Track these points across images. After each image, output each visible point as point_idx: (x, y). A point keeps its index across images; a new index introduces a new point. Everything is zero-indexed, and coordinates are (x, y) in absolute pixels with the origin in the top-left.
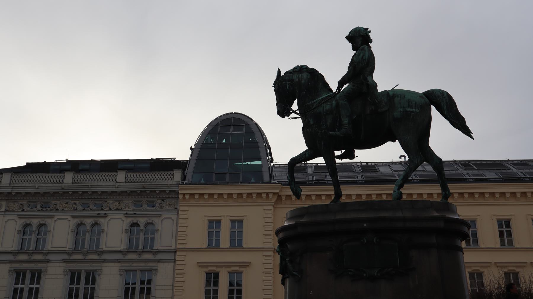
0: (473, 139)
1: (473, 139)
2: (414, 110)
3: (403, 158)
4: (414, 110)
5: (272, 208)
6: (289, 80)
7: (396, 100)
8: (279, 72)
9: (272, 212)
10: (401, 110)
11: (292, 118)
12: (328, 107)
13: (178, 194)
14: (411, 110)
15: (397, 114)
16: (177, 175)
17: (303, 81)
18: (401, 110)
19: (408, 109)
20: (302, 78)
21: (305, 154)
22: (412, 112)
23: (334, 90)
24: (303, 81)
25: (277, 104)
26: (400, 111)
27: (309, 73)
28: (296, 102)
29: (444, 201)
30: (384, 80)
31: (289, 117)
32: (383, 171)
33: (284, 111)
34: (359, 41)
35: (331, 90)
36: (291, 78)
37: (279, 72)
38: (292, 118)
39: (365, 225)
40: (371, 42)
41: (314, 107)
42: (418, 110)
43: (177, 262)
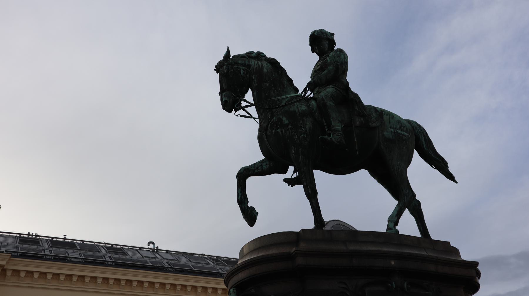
0: (456, 182)
1: (456, 182)
2: (406, 134)
3: (151, 245)
4: (406, 134)
6: (244, 65)
7: (386, 117)
8: (228, 52)
10: (392, 130)
11: (241, 116)
12: (304, 108)
14: (403, 133)
17: (265, 70)
19: (400, 132)
21: (262, 166)
22: (405, 135)
25: (220, 94)
31: (237, 114)
32: (135, 256)
33: (231, 102)
34: (326, 43)
35: (297, 90)
36: (247, 62)
37: (228, 52)
38: (241, 116)
41: (283, 104)
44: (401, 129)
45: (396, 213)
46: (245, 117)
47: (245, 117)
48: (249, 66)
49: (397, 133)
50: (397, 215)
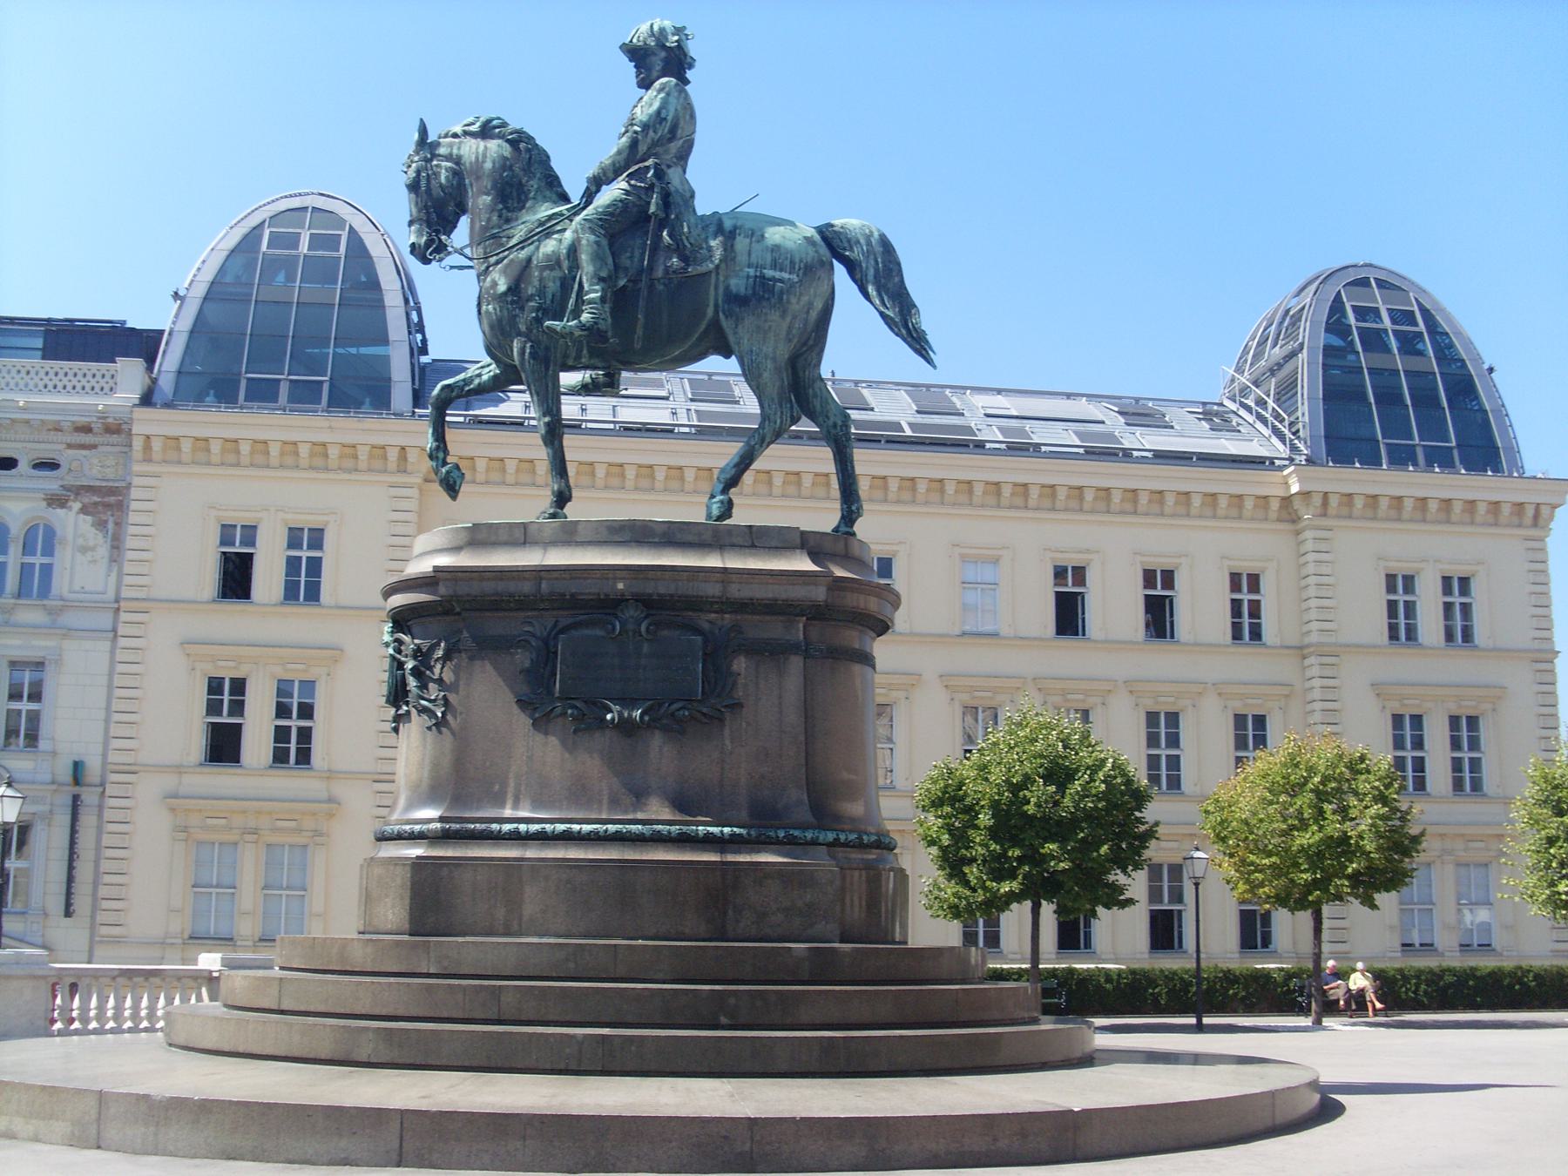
2: (786, 276)
5: (414, 492)
6: (448, 158)
8: (423, 131)
9: (412, 505)
13: (129, 434)
14: (777, 274)
15: (738, 284)
16: (129, 373)
18: (752, 272)
19: (769, 273)
20: (485, 156)
22: (781, 281)
23: (575, 191)
24: (488, 165)
26: (748, 277)
27: (508, 141)
28: (464, 222)
29: (844, 529)
30: (713, 183)
31: (444, 263)
35: (565, 198)
36: (455, 151)
39: (620, 586)
40: (691, 66)
41: (514, 241)
42: (794, 278)
43: (122, 642)
44: (774, 266)
45: (736, 460)
46: (461, 268)
47: (461, 268)
48: (458, 161)
49: (763, 277)
50: (736, 465)
